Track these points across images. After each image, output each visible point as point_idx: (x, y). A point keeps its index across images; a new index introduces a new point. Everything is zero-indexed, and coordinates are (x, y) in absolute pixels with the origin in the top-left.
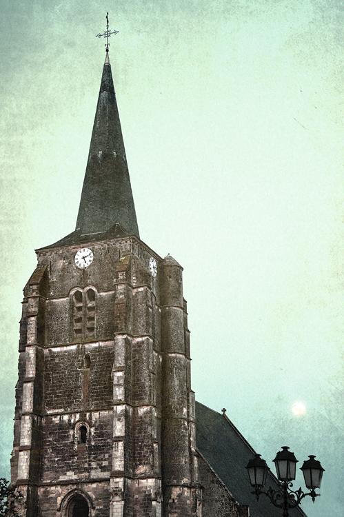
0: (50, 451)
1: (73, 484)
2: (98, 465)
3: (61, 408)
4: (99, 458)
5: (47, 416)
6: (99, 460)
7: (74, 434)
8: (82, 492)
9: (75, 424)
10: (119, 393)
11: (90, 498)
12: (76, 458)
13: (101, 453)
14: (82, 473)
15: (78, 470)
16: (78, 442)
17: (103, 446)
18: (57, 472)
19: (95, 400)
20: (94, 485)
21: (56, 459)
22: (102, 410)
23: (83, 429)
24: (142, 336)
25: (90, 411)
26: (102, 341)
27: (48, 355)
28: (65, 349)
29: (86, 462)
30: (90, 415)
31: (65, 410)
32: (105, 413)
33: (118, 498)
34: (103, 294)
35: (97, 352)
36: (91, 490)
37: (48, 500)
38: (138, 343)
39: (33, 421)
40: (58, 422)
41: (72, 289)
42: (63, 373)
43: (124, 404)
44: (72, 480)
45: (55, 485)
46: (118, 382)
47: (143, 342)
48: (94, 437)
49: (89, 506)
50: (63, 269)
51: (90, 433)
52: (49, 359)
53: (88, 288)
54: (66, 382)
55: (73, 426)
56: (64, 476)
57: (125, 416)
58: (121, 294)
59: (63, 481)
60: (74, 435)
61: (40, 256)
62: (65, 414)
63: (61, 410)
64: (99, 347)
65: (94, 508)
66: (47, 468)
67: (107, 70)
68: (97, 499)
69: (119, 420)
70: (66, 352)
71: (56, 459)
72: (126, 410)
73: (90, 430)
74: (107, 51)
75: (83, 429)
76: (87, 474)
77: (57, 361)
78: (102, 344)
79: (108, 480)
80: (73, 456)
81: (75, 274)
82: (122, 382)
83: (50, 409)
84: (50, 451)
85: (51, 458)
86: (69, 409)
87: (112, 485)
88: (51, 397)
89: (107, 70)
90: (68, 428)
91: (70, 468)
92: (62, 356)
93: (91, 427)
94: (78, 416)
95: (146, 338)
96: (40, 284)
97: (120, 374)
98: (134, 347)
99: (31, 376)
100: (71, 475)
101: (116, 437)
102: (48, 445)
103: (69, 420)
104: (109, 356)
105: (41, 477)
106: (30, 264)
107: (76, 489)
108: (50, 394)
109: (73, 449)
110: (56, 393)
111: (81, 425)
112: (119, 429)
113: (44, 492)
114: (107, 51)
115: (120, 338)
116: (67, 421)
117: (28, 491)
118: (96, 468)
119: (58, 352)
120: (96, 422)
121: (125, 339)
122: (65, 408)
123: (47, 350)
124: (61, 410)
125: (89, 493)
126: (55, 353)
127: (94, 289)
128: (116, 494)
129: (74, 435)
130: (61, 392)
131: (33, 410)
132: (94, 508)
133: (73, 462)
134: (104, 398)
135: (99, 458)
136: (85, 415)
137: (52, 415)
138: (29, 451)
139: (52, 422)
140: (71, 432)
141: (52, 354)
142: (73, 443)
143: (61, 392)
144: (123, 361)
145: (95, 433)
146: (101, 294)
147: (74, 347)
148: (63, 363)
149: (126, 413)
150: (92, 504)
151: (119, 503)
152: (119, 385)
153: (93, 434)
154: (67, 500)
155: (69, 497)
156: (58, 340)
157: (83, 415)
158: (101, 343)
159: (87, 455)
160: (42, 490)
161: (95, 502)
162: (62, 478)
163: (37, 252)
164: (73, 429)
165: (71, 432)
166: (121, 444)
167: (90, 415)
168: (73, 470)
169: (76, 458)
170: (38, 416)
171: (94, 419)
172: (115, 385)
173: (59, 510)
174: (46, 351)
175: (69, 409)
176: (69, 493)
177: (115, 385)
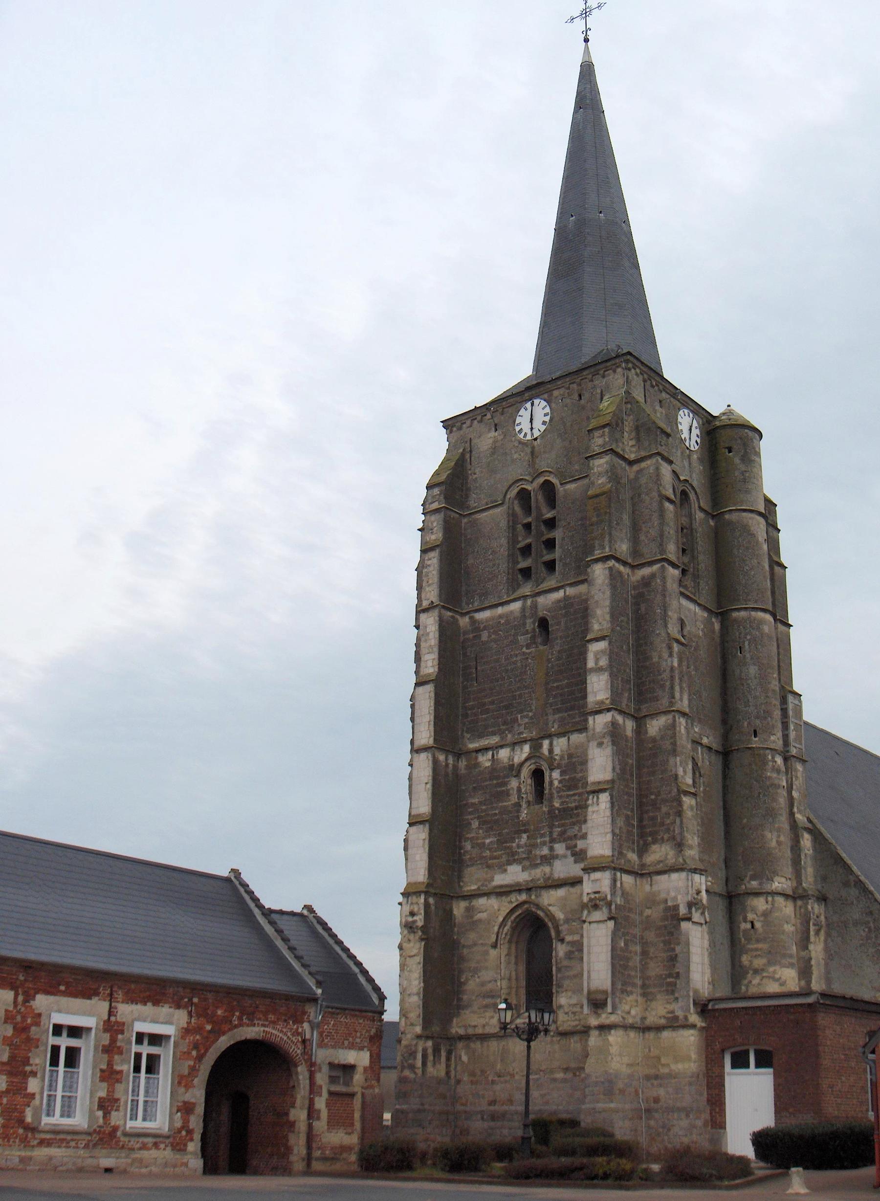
0: (475, 824)
1: (520, 891)
2: (567, 848)
3: (494, 734)
4: (570, 833)
5: (469, 752)
6: (570, 838)
7: (524, 783)
8: (538, 906)
9: (522, 764)
10: (598, 688)
11: (552, 918)
12: (525, 836)
13: (574, 824)
14: (536, 866)
15: (530, 861)
16: (528, 802)
17: (576, 808)
18: (488, 867)
19: (559, 711)
20: (561, 892)
21: (487, 841)
22: (572, 732)
23: (538, 775)
24: (651, 563)
25: (550, 736)
26: (571, 585)
27: (469, 628)
28: (500, 610)
29: (544, 843)
30: (551, 744)
31: (502, 738)
32: (576, 738)
33: (597, 915)
34: (571, 486)
35: (561, 609)
36: (552, 901)
37: (474, 925)
38: (643, 578)
39: (435, 762)
40: (488, 764)
41: (510, 486)
42: (497, 661)
43: (609, 710)
44: (518, 884)
45: (487, 894)
46: (596, 664)
47: (653, 576)
48: (559, 790)
49: (553, 934)
50: (494, 450)
51: (551, 783)
52: (471, 636)
53: (541, 480)
54: (503, 679)
55: (514, 770)
56: (503, 876)
57: (612, 736)
58: (600, 474)
59: (501, 886)
60: (519, 790)
61: (451, 432)
62: (502, 747)
63: (494, 740)
64: (566, 598)
65: (562, 940)
66: (470, 859)
67: (587, 72)
68: (567, 921)
69: (600, 745)
70: (500, 616)
71: (487, 841)
72: (614, 723)
73: (550, 776)
74: (586, 40)
75: (538, 775)
76: (547, 869)
77: (485, 636)
78: (570, 591)
79: (576, 882)
80: (519, 832)
81: (516, 456)
82: (604, 662)
83: (471, 740)
84: (475, 824)
85: (477, 838)
86: (509, 736)
87: (587, 887)
88: (475, 715)
89: (587, 72)
90: (508, 777)
91: (513, 858)
92: (495, 626)
93: (552, 770)
94: (527, 748)
95: (658, 566)
96: (451, 489)
97: (602, 645)
98: (634, 588)
99: (431, 670)
100: (515, 874)
101: (594, 783)
102: (470, 813)
103: (511, 759)
104: (579, 612)
105: (460, 877)
106: (434, 450)
107: (524, 903)
108: (472, 708)
109: (518, 817)
110: (484, 704)
111: (533, 767)
112: (600, 765)
113: (468, 909)
114: (586, 40)
115: (599, 572)
116: (506, 760)
117: (427, 905)
118: (565, 856)
119: (487, 620)
120: (562, 757)
121: (611, 569)
122: (501, 733)
123: (467, 619)
124: (494, 740)
125: (550, 908)
126: (480, 622)
127: (554, 480)
128: (596, 907)
129: (519, 790)
130: (492, 703)
131: (435, 740)
132: (562, 940)
133: (519, 846)
134: (574, 709)
135: (570, 833)
136: (541, 746)
137: (478, 751)
138: (427, 825)
139: (477, 765)
140: (514, 783)
141: (476, 627)
142: (518, 805)
143: (492, 703)
144: (608, 617)
145: (560, 782)
146: (568, 486)
147: (516, 606)
148: (495, 641)
149: (614, 733)
150: (558, 932)
151: (601, 925)
152: (599, 670)
153: (556, 783)
154: (509, 923)
155: (512, 918)
156: (485, 594)
157: (536, 746)
158: (568, 589)
159: (546, 830)
160: (463, 904)
161: (563, 928)
162: (500, 879)
163: (449, 424)
164: (518, 775)
165: (514, 783)
166: (604, 798)
167: (551, 744)
168: (518, 861)
169: (525, 836)
170: (447, 752)
171: (557, 751)
172: (592, 670)
173: (495, 946)
174: (464, 622)
175: (509, 736)
176: (512, 911)
177: (592, 670)
